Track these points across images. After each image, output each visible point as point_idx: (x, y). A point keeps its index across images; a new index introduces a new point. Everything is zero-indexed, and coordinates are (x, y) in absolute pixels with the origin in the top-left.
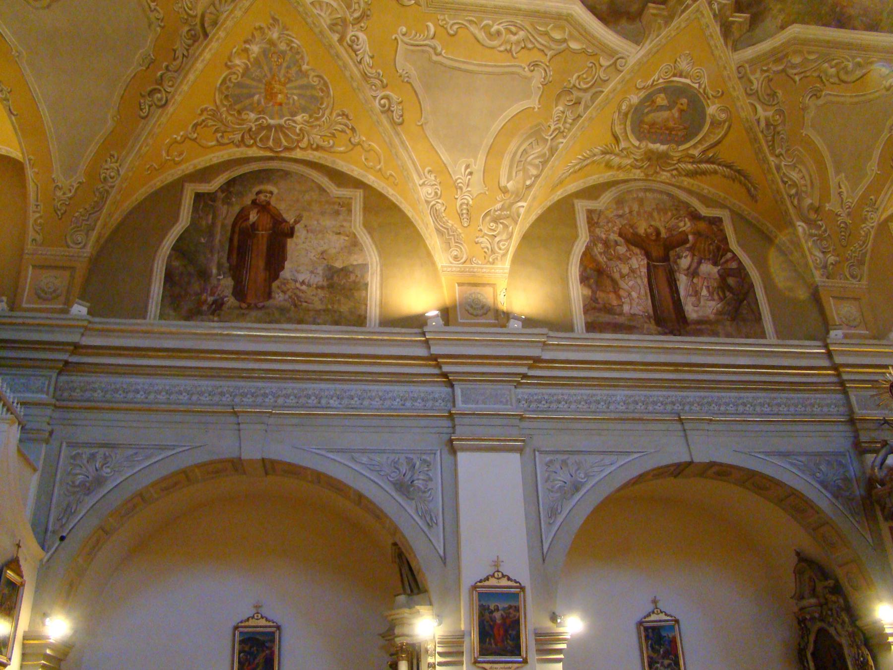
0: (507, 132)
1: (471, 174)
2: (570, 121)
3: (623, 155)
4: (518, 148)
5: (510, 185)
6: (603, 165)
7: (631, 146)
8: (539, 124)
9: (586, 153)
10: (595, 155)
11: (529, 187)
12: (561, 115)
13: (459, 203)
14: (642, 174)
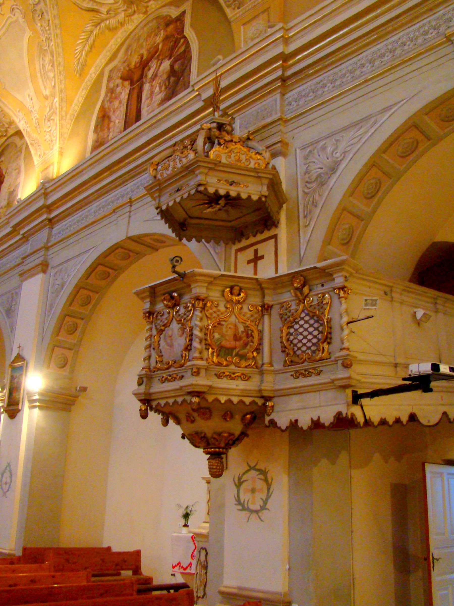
0: (31, 61)
1: (32, 99)
2: (47, 28)
3: (112, 15)
4: (40, 66)
5: (47, 92)
6: (107, 31)
7: (110, 6)
8: (39, 43)
9: (83, 36)
10: (92, 32)
11: (54, 87)
12: (42, 29)
13: (34, 120)
14: (141, 15)
